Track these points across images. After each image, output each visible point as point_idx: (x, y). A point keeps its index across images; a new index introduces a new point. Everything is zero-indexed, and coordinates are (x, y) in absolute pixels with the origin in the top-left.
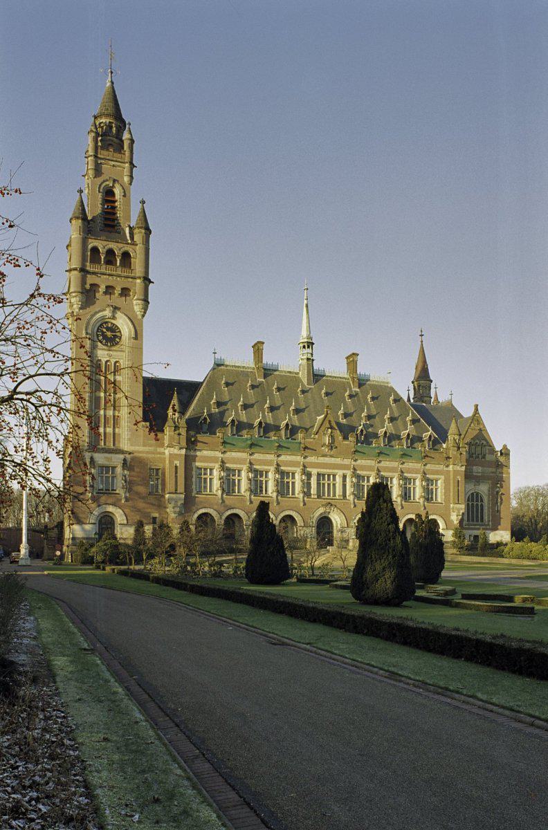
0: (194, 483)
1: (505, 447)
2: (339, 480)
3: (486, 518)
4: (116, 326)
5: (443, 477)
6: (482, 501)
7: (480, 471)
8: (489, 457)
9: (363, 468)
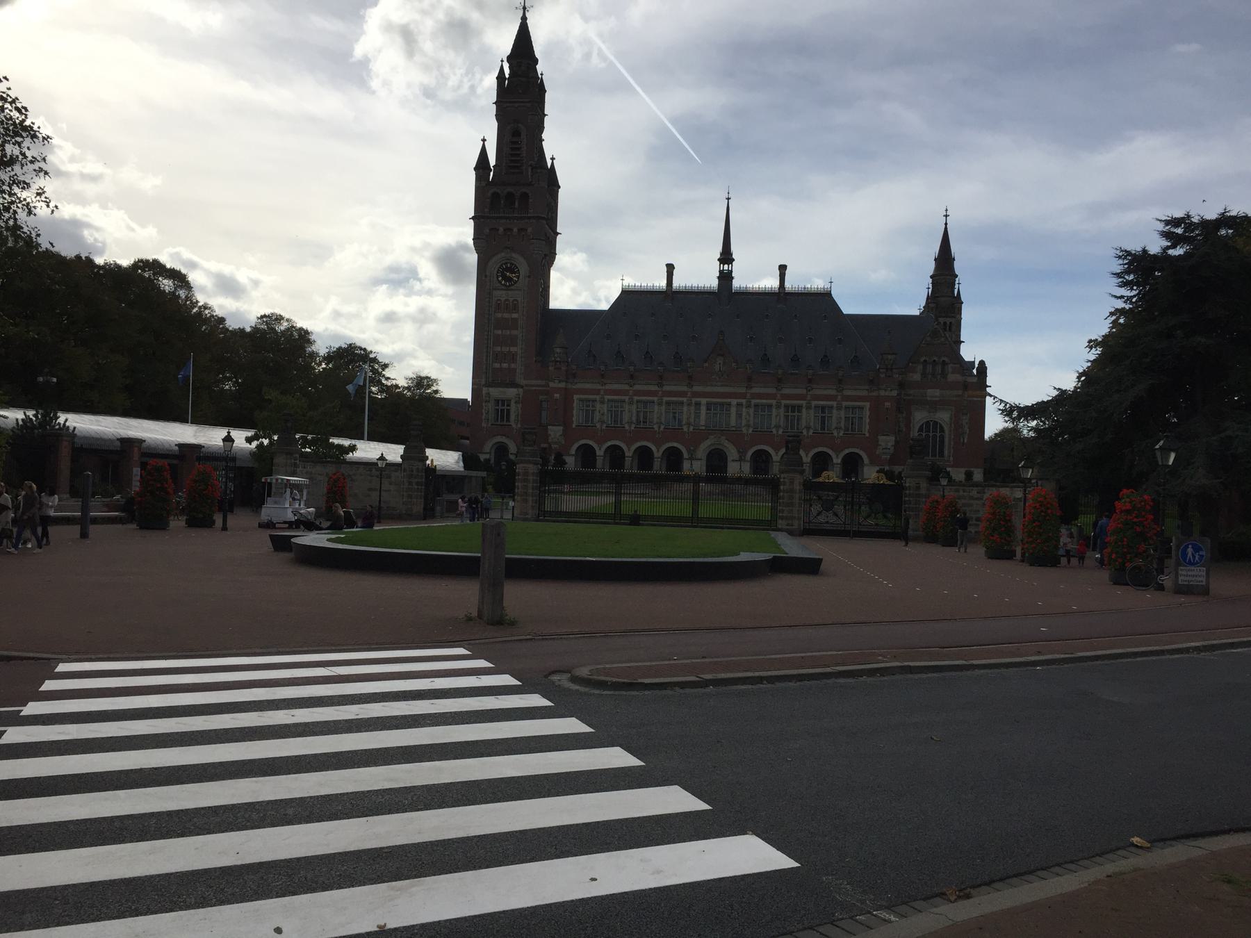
0: (575, 415)
1: (982, 363)
2: (733, 410)
3: (946, 452)
4: (515, 266)
5: (868, 404)
6: (942, 430)
7: (938, 394)
8: (952, 377)
9: (760, 396)
